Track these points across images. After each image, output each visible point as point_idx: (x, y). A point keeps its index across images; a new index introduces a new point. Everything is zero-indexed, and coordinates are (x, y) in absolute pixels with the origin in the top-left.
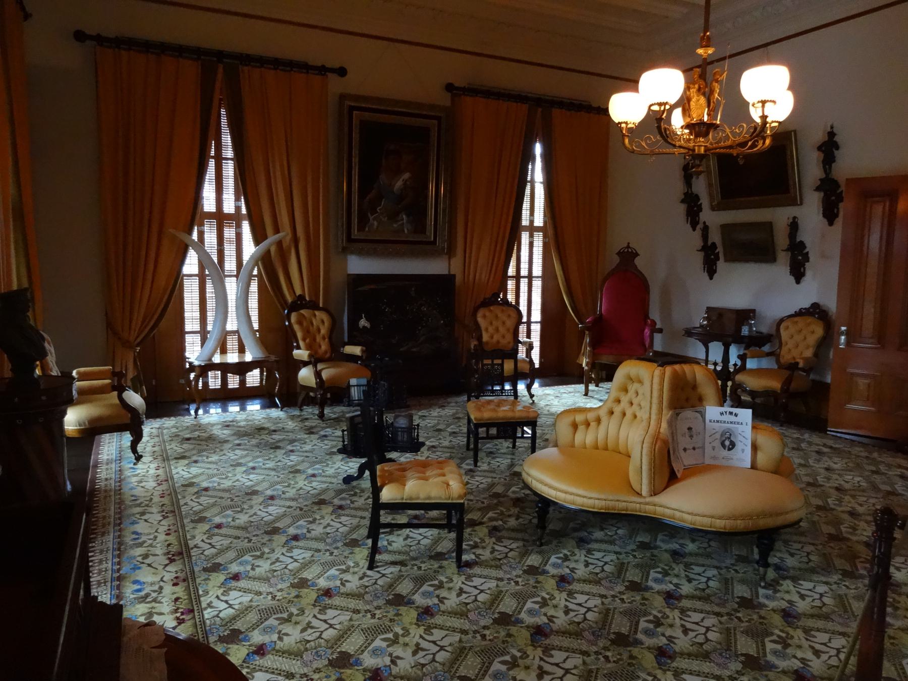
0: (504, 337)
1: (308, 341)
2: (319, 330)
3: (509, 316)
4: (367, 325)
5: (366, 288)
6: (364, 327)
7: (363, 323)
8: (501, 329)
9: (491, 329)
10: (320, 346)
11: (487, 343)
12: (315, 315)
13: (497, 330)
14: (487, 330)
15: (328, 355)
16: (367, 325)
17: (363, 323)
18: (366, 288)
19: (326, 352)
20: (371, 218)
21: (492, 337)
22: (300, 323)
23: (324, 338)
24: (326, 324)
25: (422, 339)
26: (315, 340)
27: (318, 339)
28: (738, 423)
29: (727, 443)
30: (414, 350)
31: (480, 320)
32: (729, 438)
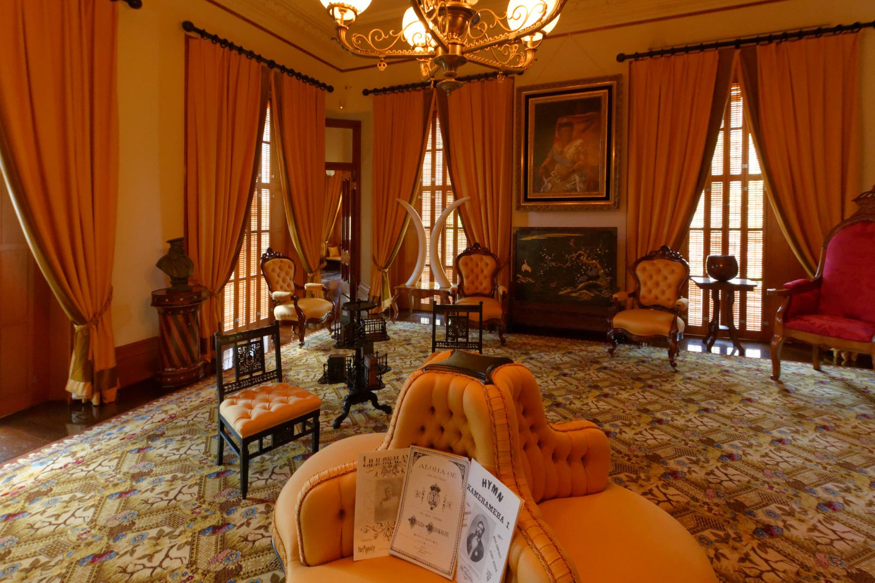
0: (663, 292)
1: (470, 278)
2: (482, 271)
3: (673, 271)
5: (529, 238)
6: (526, 271)
8: (663, 285)
9: (650, 284)
10: (481, 284)
11: (644, 297)
12: (482, 259)
13: (657, 284)
14: (645, 284)
15: (487, 292)
17: (525, 267)
18: (529, 238)
19: (485, 289)
20: (546, 181)
21: (650, 291)
22: (466, 264)
23: (485, 277)
24: (489, 267)
25: (581, 285)
26: (477, 277)
27: (481, 277)
28: (499, 515)
29: (475, 543)
30: (574, 295)
31: (639, 273)
32: (480, 536)
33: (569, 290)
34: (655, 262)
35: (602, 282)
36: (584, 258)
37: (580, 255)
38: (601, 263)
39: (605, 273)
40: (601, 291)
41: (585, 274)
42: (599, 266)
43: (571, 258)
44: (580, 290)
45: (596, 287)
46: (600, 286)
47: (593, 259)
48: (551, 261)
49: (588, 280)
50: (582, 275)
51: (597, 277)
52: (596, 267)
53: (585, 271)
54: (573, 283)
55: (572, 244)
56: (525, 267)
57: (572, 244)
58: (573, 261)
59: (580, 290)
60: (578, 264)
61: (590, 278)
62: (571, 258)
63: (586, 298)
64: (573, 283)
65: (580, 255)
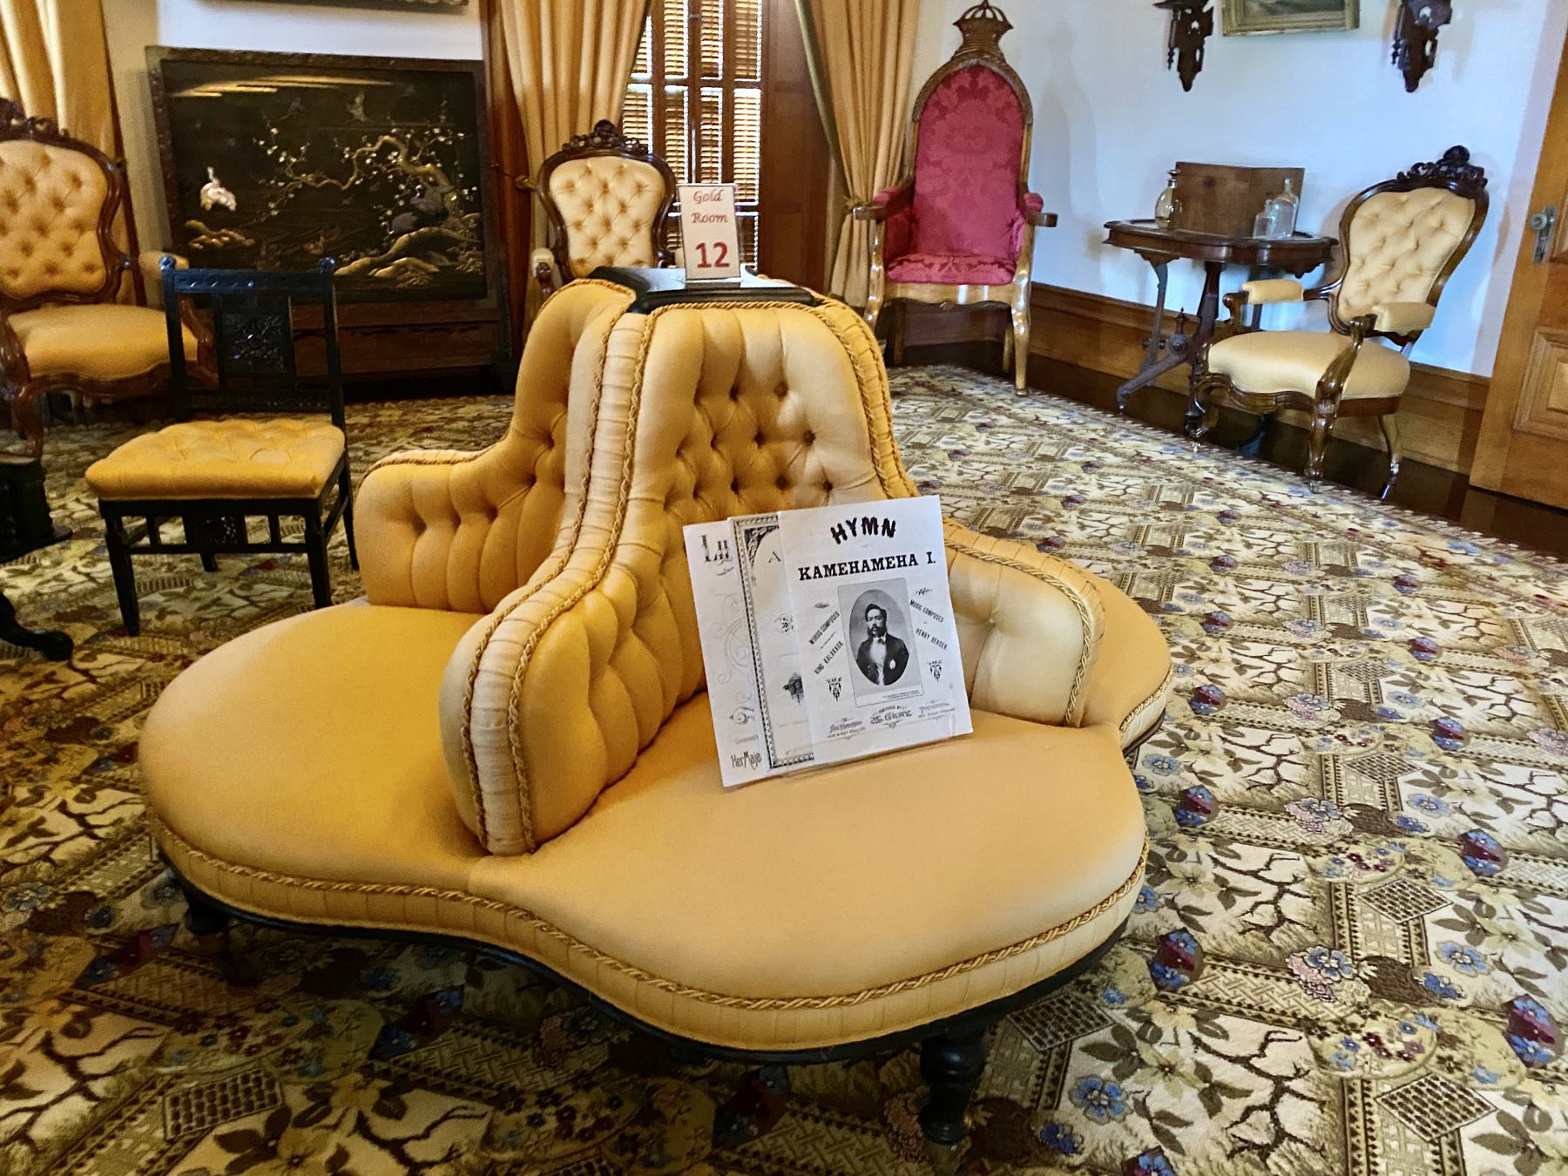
4: (228, 200)
6: (217, 206)
7: (213, 192)
16: (228, 200)
30: (381, 272)
34: (590, 163)
35: (460, 227)
37: (387, 148)
38: (447, 170)
39: (463, 204)
40: (453, 257)
41: (409, 207)
42: (443, 181)
43: (362, 158)
45: (440, 244)
46: (456, 242)
47: (424, 161)
48: (297, 169)
49: (417, 226)
50: (398, 211)
51: (441, 216)
52: (435, 184)
53: (407, 198)
54: (375, 241)
56: (213, 192)
58: (368, 169)
60: (382, 176)
61: (423, 219)
62: (362, 158)
64: (375, 241)
65: (387, 148)
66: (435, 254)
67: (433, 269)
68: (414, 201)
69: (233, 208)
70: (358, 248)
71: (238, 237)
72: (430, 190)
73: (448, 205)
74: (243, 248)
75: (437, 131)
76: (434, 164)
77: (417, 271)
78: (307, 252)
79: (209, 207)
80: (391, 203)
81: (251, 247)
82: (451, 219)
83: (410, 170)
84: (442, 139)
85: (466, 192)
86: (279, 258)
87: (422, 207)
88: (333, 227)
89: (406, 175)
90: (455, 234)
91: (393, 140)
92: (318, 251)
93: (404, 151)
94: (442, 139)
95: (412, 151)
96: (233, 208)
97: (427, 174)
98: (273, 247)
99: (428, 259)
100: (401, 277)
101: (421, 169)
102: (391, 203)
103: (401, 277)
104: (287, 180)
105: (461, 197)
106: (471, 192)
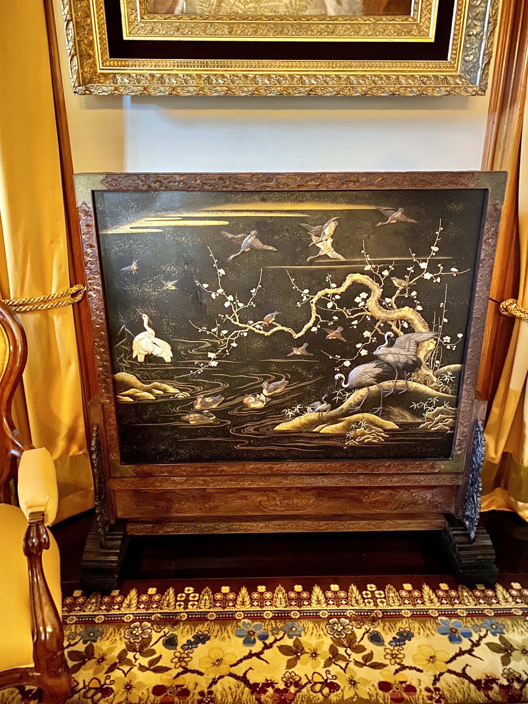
4: (164, 351)
16: (164, 351)
30: (328, 429)
33: (310, 416)
36: (371, 304)
37: (358, 288)
40: (419, 413)
44: (348, 413)
45: (404, 399)
47: (401, 303)
49: (380, 378)
51: (411, 368)
52: (410, 330)
55: (325, 246)
56: (147, 344)
57: (325, 246)
59: (348, 413)
61: (390, 372)
62: (322, 302)
63: (369, 438)
66: (396, 410)
67: (391, 425)
68: (381, 351)
69: (168, 359)
70: (304, 399)
71: (171, 390)
72: (402, 337)
73: (422, 355)
74: (177, 402)
75: (424, 265)
76: (413, 306)
77: (372, 428)
78: (246, 406)
79: (141, 359)
80: (350, 352)
81: (186, 400)
82: (424, 371)
83: (380, 314)
84: (428, 276)
85: (447, 339)
86: (214, 412)
87: (390, 358)
88: (279, 379)
89: (374, 320)
90: (422, 387)
91: (364, 279)
92: (259, 405)
93: (377, 291)
94: (428, 276)
95: (388, 290)
96: (168, 359)
97: (399, 321)
98: (209, 400)
99: (386, 415)
100: (352, 434)
101: (397, 313)
102: (350, 352)
103: (352, 434)
104: (232, 328)
105: (441, 346)
106: (454, 339)
